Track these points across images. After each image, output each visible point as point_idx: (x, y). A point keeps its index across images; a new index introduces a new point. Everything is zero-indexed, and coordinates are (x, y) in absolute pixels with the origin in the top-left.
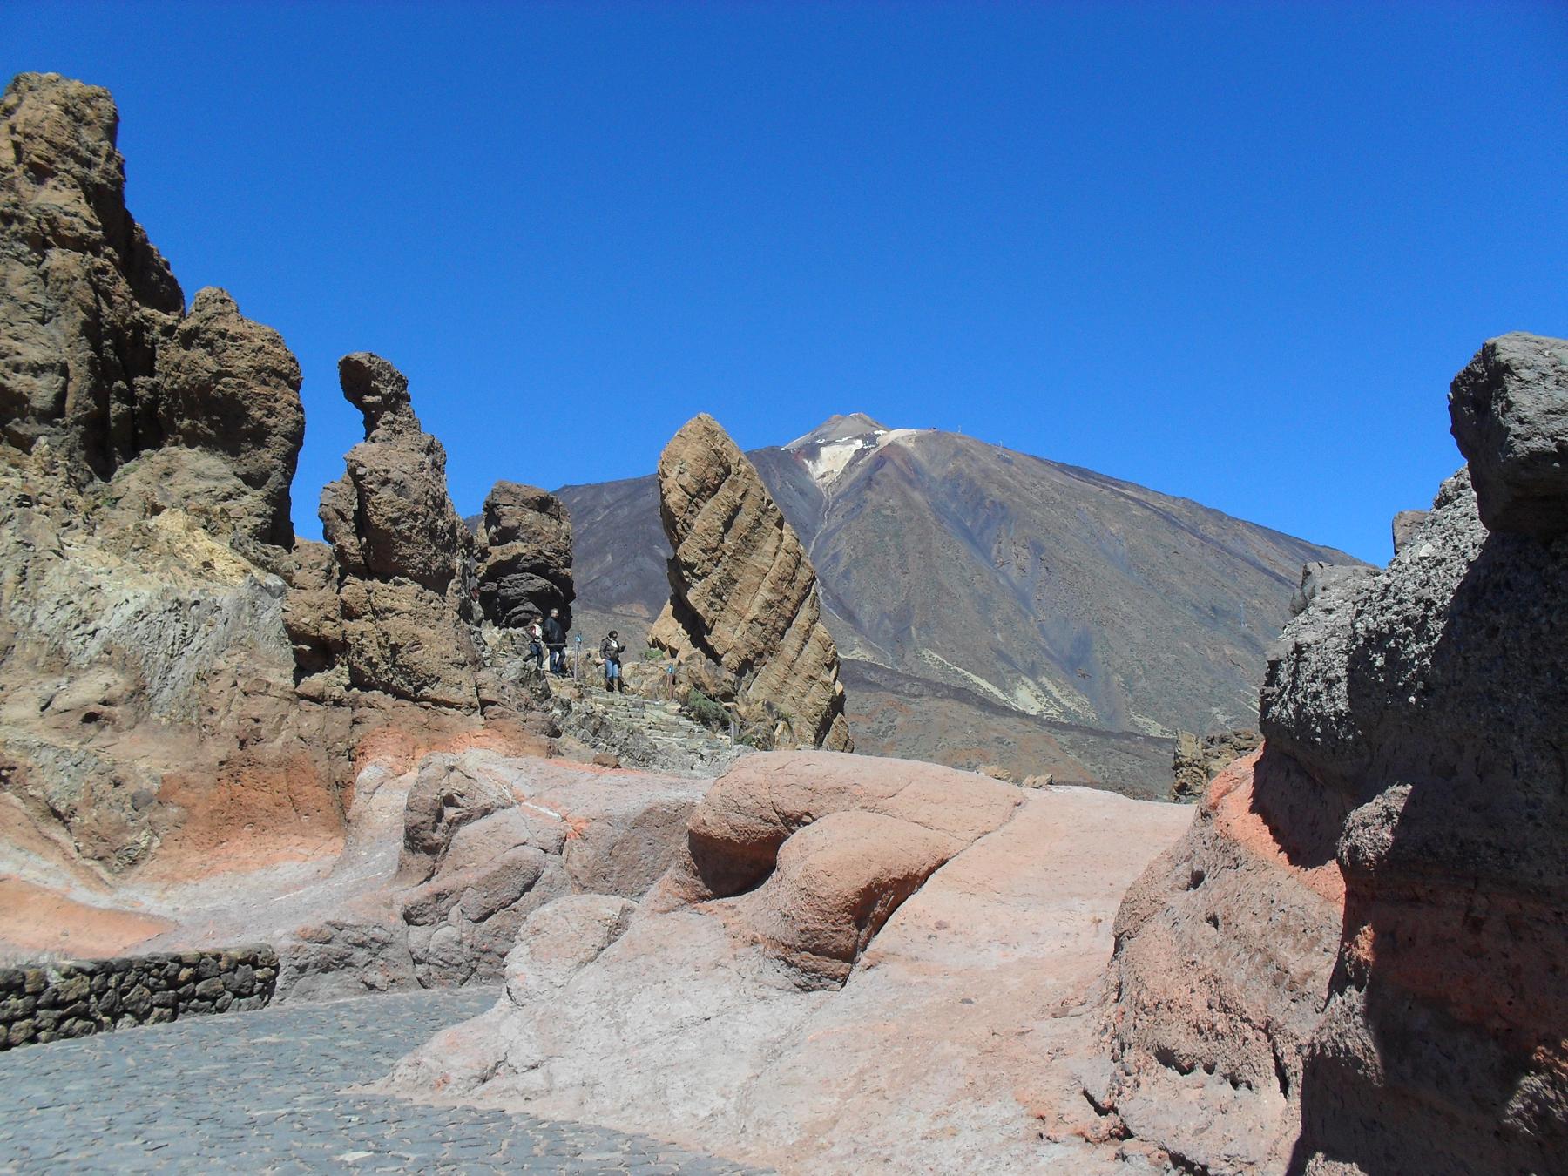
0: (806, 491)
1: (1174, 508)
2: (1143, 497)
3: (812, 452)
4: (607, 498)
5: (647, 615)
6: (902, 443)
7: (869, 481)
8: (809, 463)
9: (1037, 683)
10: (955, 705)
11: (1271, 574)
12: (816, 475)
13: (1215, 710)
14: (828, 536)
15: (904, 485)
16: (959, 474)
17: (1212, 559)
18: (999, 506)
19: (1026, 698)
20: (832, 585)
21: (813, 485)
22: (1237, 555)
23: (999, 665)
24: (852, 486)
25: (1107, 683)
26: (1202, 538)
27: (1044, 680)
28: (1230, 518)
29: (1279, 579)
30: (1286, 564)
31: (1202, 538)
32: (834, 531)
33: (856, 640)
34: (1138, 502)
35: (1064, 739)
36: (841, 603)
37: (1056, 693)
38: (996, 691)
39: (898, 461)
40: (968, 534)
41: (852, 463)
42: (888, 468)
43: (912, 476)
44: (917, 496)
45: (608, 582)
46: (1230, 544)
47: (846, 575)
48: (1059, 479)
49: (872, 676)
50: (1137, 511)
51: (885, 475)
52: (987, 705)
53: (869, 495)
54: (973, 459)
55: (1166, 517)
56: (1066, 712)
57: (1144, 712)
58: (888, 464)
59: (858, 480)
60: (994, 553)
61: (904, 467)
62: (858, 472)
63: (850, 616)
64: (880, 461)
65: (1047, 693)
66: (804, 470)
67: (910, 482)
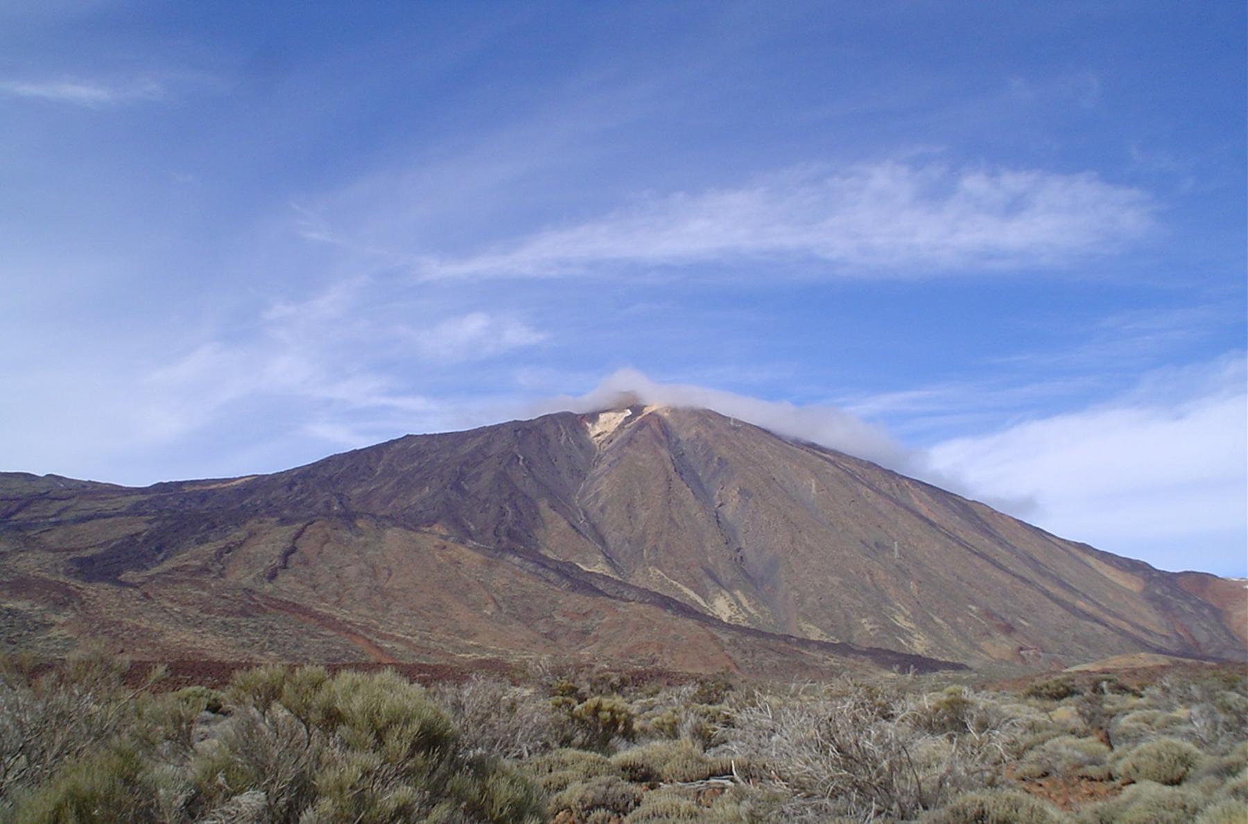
0: (586, 447)
3: (593, 417)
5: (445, 533)
6: (660, 413)
7: (630, 441)
8: (589, 425)
9: (732, 595)
10: (653, 609)
12: (593, 434)
13: (864, 620)
15: (655, 443)
19: (722, 608)
21: (590, 442)
23: (708, 581)
24: (618, 443)
25: (786, 597)
27: (738, 593)
28: (903, 477)
29: (932, 524)
33: (600, 557)
35: (726, 638)
37: (745, 603)
38: (700, 600)
41: (621, 427)
42: (646, 431)
44: (664, 453)
47: (602, 510)
49: (601, 586)
50: (831, 469)
52: (686, 610)
53: (626, 449)
56: (750, 618)
57: (809, 620)
59: (623, 439)
60: (716, 497)
62: (625, 432)
64: (641, 425)
65: (738, 602)
67: (660, 442)
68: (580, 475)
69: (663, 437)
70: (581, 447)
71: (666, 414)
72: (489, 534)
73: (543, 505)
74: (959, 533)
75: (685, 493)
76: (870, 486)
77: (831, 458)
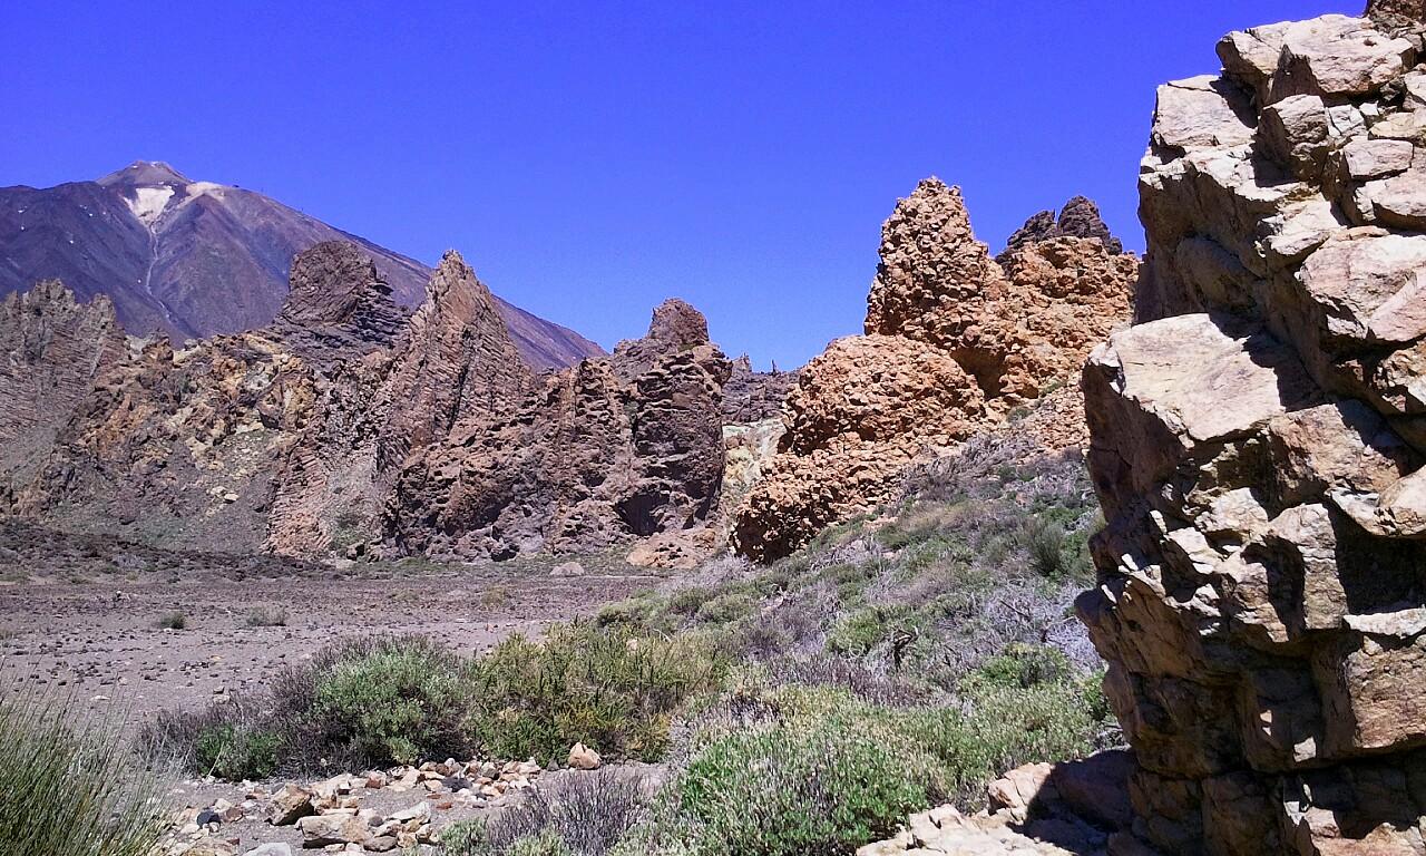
0: (132, 225)
2: (418, 268)
8: (129, 202)
11: (527, 341)
14: (162, 268)
16: (269, 228)
20: (176, 309)
21: (137, 222)
34: (416, 271)
36: (188, 326)
43: (231, 226)
44: (238, 242)
47: (187, 302)
54: (280, 217)
59: (178, 221)
61: (220, 216)
66: (125, 205)
68: (141, 263)
70: (130, 227)
71: (221, 198)
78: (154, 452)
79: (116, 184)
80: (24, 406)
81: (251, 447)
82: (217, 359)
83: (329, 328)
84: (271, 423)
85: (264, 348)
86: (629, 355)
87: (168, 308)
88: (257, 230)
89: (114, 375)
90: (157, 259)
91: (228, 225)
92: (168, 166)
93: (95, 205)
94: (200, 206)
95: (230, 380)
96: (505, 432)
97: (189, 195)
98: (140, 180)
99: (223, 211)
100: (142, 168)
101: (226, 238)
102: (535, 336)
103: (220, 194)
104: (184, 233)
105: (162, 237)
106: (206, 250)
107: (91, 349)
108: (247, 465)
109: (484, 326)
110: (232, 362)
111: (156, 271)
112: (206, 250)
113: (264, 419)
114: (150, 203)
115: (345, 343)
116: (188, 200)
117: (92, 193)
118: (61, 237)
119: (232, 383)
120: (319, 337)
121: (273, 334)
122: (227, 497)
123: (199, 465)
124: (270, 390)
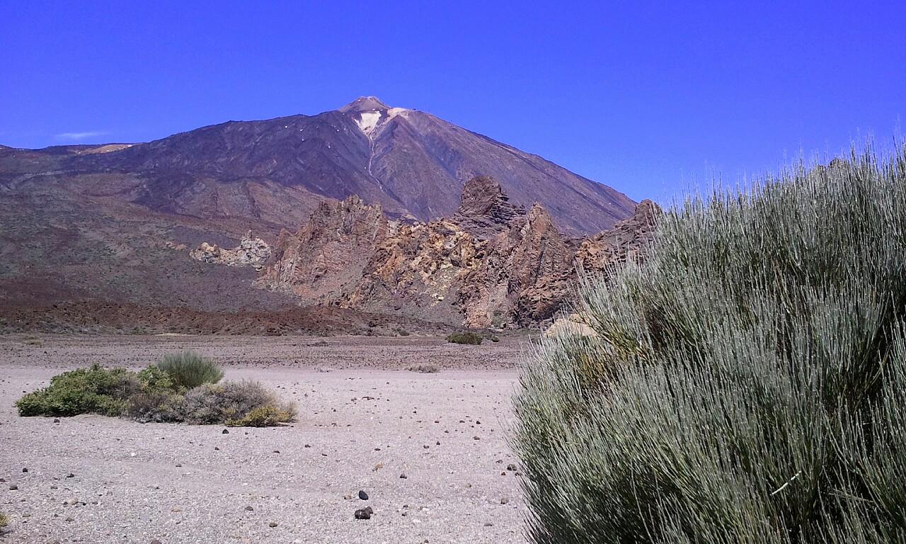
0: (360, 136)
1: (533, 159)
4: (258, 130)
6: (402, 116)
8: (357, 122)
11: (581, 194)
15: (410, 137)
16: (433, 134)
17: (553, 185)
18: (456, 152)
20: (385, 183)
22: (564, 184)
26: (548, 175)
29: (584, 197)
30: (586, 189)
31: (548, 175)
32: (379, 158)
34: (516, 155)
36: (392, 193)
39: (403, 125)
40: (441, 163)
41: (378, 124)
42: (399, 128)
43: (412, 133)
45: (281, 174)
46: (560, 178)
47: (391, 179)
48: (479, 140)
51: (399, 131)
54: (439, 127)
55: (530, 163)
58: (399, 126)
60: (457, 175)
61: (406, 127)
63: (398, 200)
66: (355, 124)
69: (412, 133)
71: (406, 117)
72: (337, 194)
73: (356, 175)
74: (600, 203)
75: (441, 172)
76: (543, 171)
77: (514, 152)
78: (409, 277)
79: (349, 111)
80: (346, 255)
81: (448, 275)
82: (431, 234)
83: (480, 218)
84: (456, 264)
85: (452, 228)
86: (622, 229)
87: (381, 183)
88: (427, 135)
89: (388, 243)
90: (373, 155)
91: (412, 133)
92: (378, 100)
93: (339, 125)
94: (396, 123)
95: (437, 244)
96: (557, 283)
97: (389, 116)
98: (363, 108)
99: (408, 125)
100: (363, 101)
101: (411, 142)
102: (586, 191)
103: (406, 115)
104: (388, 139)
105: (376, 142)
106: (400, 148)
107: (373, 227)
108: (446, 283)
109: (550, 234)
110: (438, 236)
111: (374, 162)
112: (400, 148)
113: (452, 262)
114: (369, 122)
115: (488, 225)
116: (389, 119)
117: (338, 118)
118: (323, 143)
119: (438, 245)
120: (476, 222)
121: (455, 221)
122: (439, 298)
123: (426, 283)
124: (455, 248)
